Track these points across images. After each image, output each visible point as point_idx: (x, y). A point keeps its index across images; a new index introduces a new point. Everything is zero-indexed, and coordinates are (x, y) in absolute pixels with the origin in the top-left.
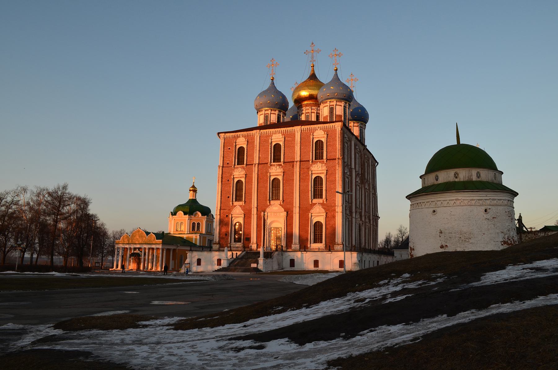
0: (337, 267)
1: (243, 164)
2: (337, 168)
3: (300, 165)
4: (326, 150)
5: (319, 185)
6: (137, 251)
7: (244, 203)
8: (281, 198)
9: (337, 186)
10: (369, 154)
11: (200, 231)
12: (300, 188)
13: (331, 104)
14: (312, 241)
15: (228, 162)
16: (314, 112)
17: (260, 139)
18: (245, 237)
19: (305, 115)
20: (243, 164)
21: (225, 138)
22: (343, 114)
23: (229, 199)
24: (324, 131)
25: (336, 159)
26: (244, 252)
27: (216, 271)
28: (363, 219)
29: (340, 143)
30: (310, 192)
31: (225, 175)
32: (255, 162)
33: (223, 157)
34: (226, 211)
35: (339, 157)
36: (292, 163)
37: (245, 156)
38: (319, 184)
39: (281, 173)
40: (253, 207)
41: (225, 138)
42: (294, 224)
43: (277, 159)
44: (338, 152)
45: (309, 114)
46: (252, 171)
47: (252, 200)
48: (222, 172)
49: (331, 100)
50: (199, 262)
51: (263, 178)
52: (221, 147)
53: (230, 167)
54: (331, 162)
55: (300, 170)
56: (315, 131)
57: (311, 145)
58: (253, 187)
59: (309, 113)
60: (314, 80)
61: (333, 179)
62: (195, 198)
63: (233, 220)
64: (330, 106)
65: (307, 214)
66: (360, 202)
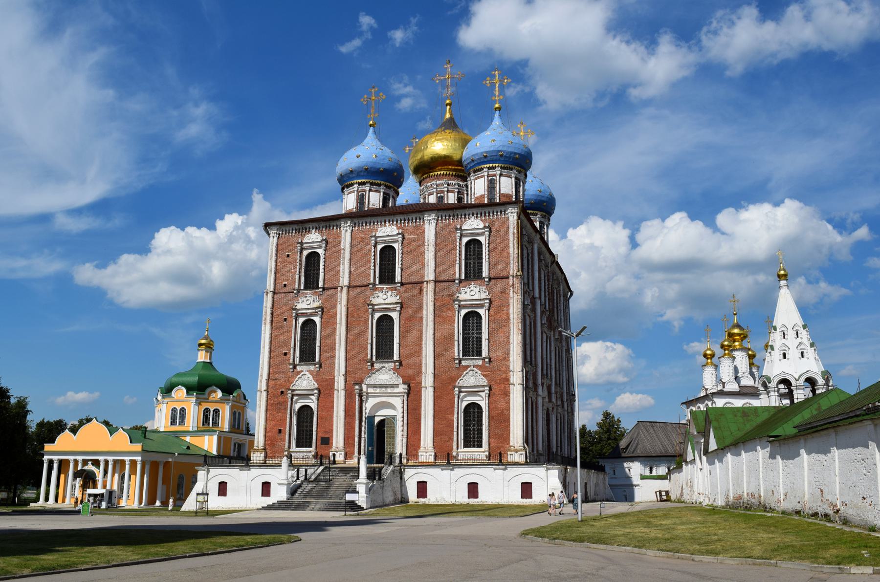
0: (514, 497)
1: (318, 288)
2: (511, 295)
3: (435, 290)
4: (487, 260)
5: (473, 330)
6: (90, 467)
7: (317, 366)
8: (396, 357)
9: (512, 331)
10: (560, 274)
11: (220, 426)
12: (434, 334)
13: (492, 172)
14: (461, 443)
15: (286, 283)
16: (453, 192)
17: (352, 237)
18: (320, 435)
19: (435, 196)
20: (318, 288)
22: (514, 193)
23: (287, 358)
24: (484, 222)
25: (508, 278)
26: (322, 468)
27: (264, 508)
28: (554, 400)
29: (516, 246)
30: (456, 343)
31: (279, 310)
32: (341, 281)
33: (276, 273)
34: (278, 382)
35: (515, 272)
36: (419, 284)
37: (321, 271)
38: (473, 326)
39: (395, 306)
41: (279, 234)
43: (387, 276)
44: (512, 262)
45: (442, 195)
46: (336, 301)
47: (334, 360)
48: (273, 303)
49: (491, 165)
50: (223, 488)
52: (272, 252)
53: (289, 293)
54: (498, 284)
55: (435, 299)
56: (465, 221)
57: (456, 250)
58: (338, 333)
59: (442, 192)
60: (453, 130)
61: (504, 317)
62: (208, 361)
63: (311, 397)
64: (488, 177)
65: (451, 387)
66: (549, 366)
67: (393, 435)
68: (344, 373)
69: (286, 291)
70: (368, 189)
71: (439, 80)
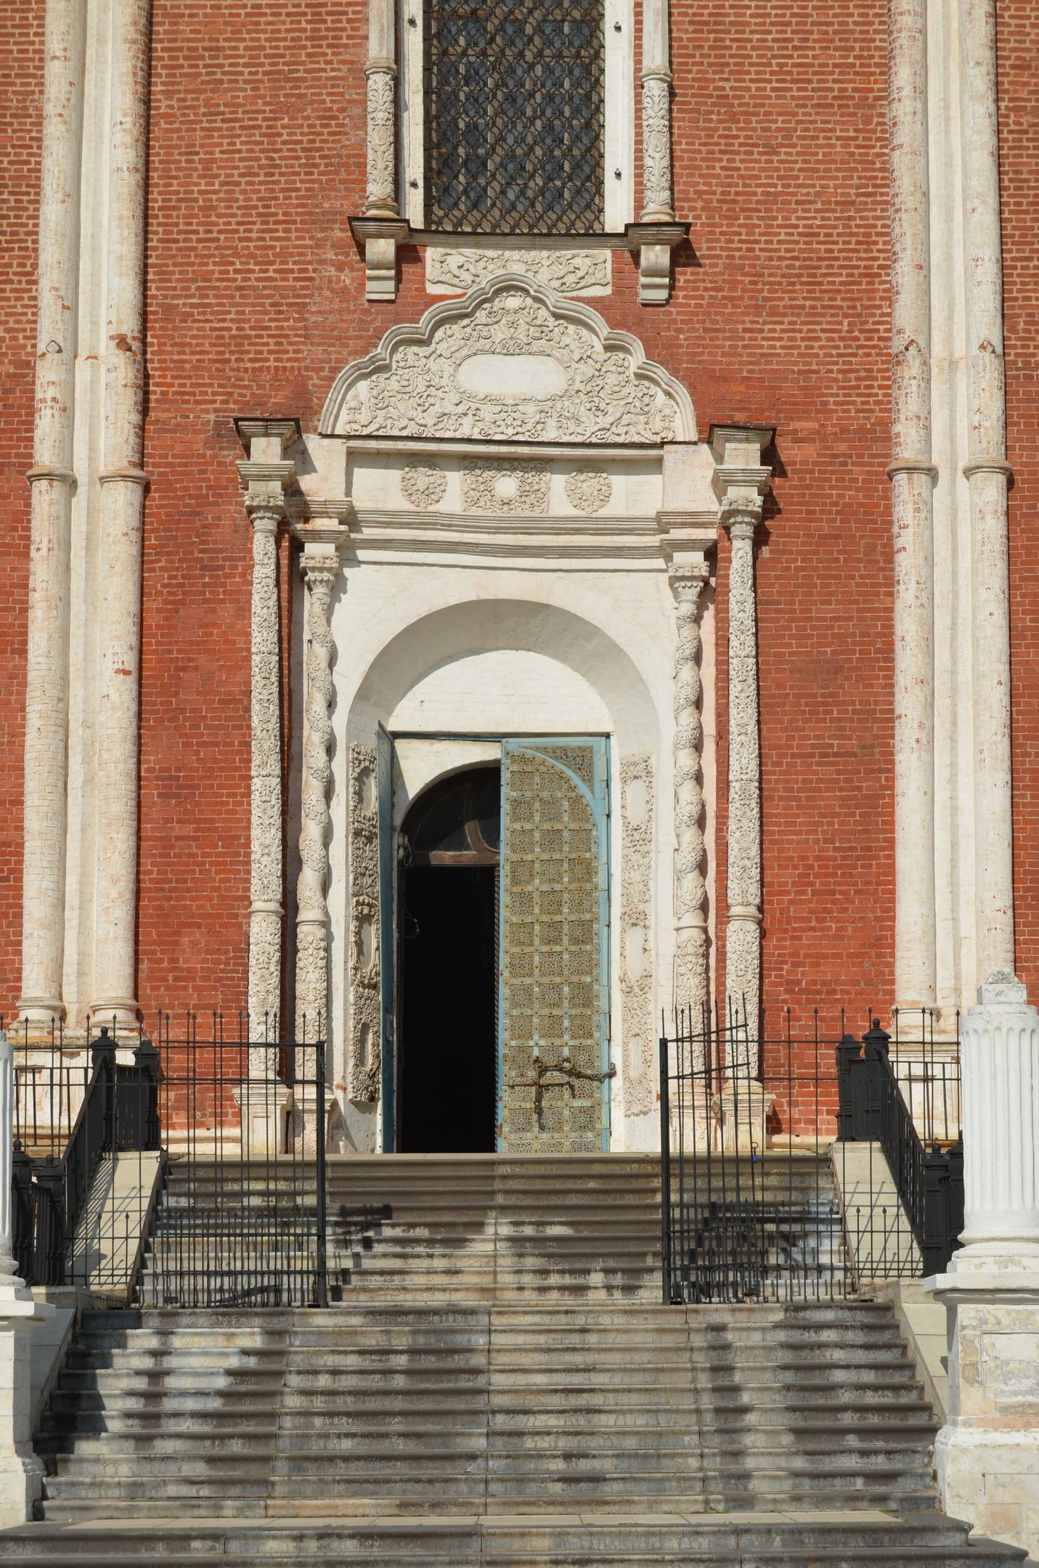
40: (49, 327)
42: (907, 662)
67: (578, 906)
68: (130, 326)
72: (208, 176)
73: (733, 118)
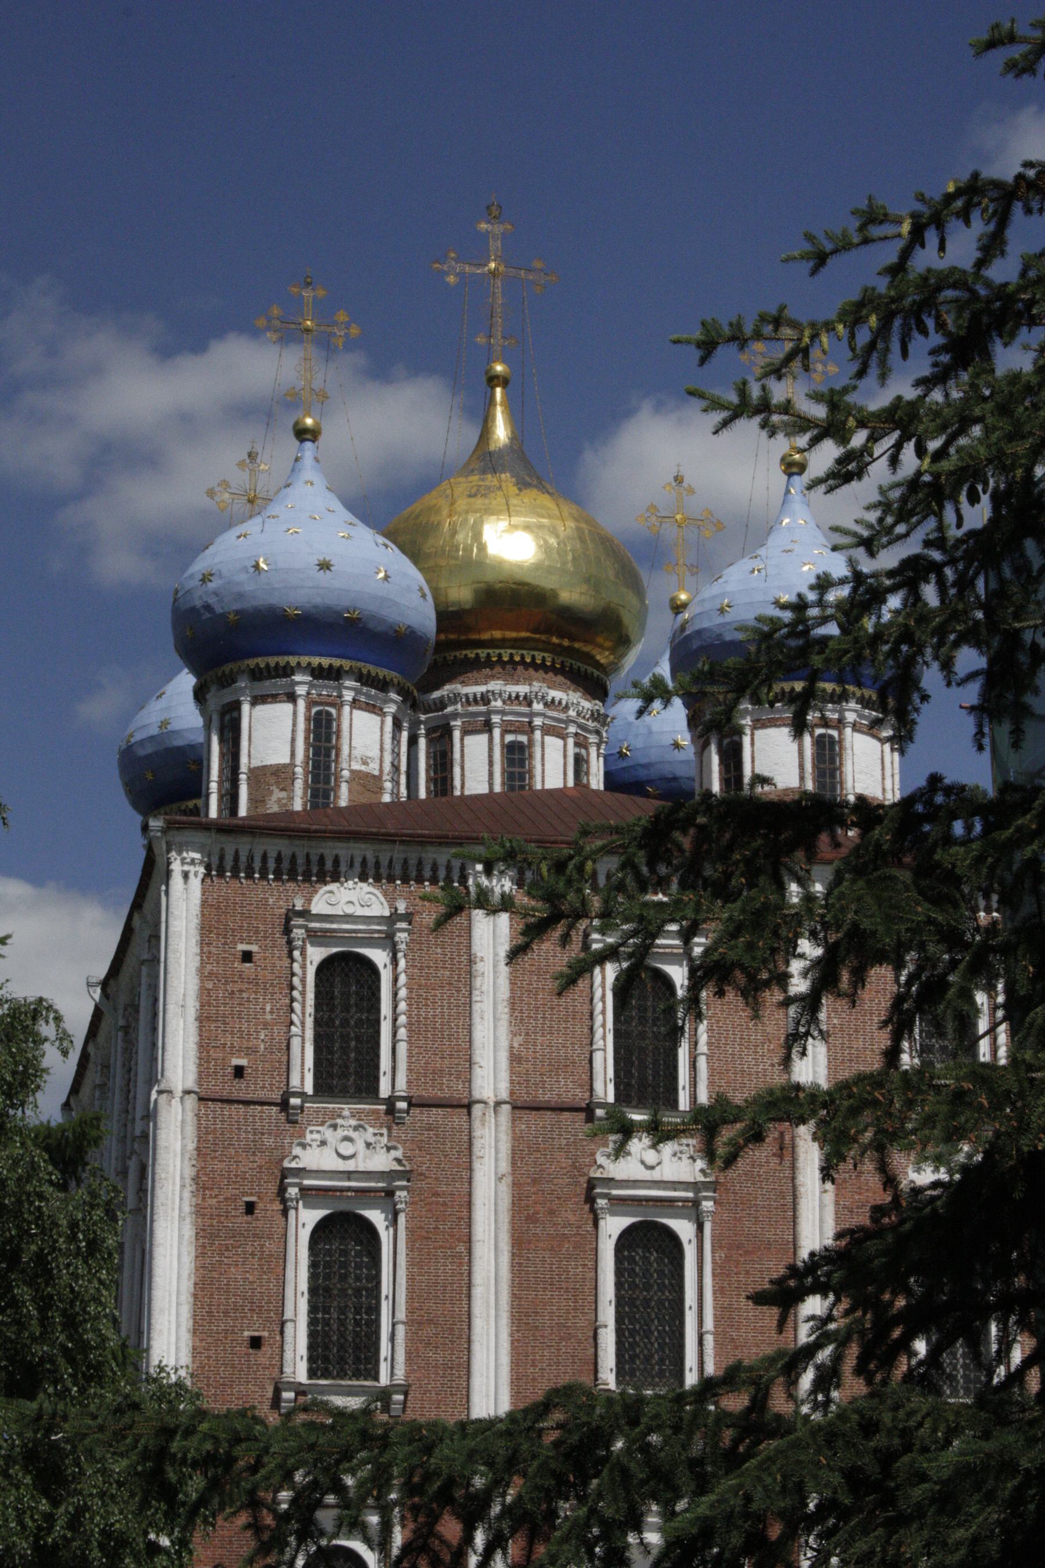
15: (243, 1062)
21: (208, 868)
31: (220, 1166)
45: (523, 739)
51: (552, 1212)
53: (262, 1103)
69: (242, 1096)
70: (348, 695)
71: (457, 275)
72: (534, 1366)
73: (736, 1348)
